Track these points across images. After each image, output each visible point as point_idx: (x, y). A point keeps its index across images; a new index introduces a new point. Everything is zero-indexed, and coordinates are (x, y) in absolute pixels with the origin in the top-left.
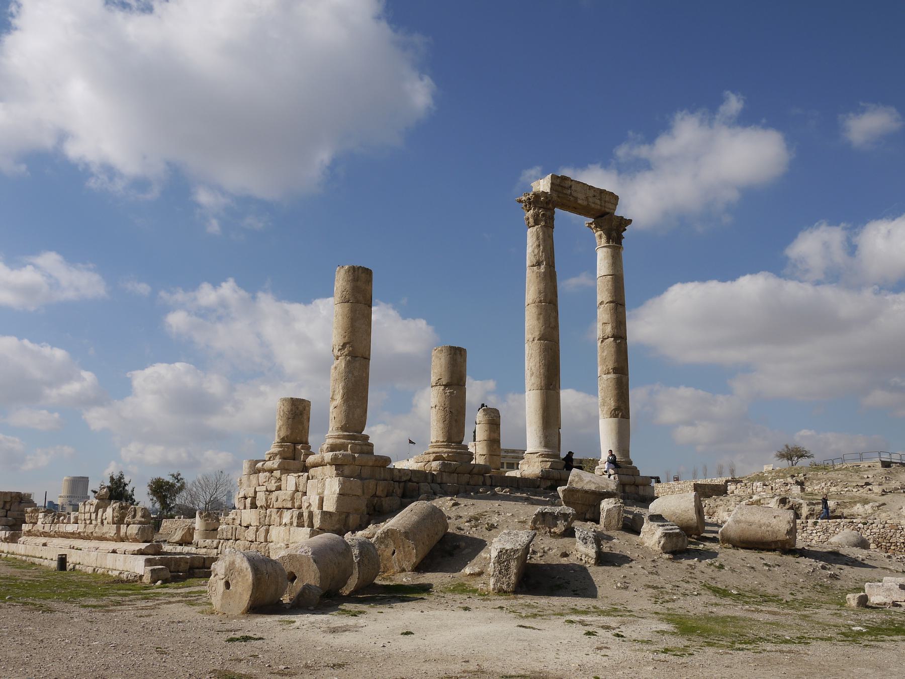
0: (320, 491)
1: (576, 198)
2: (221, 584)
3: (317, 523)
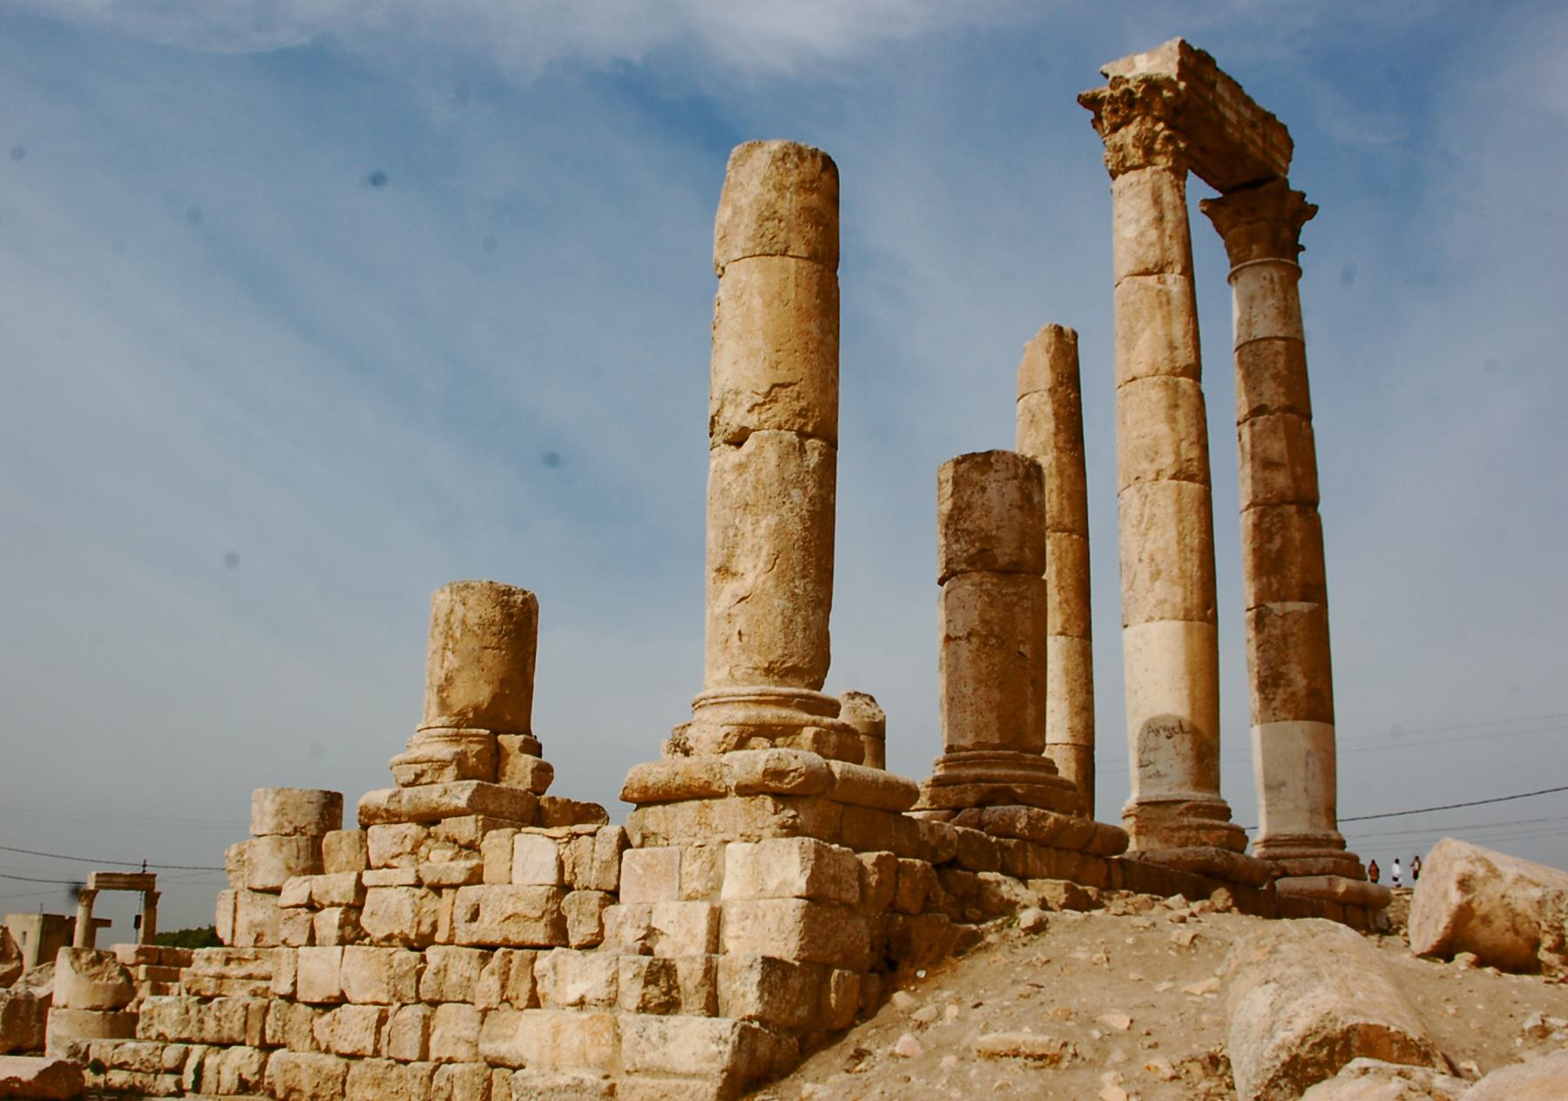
0: (698, 885)
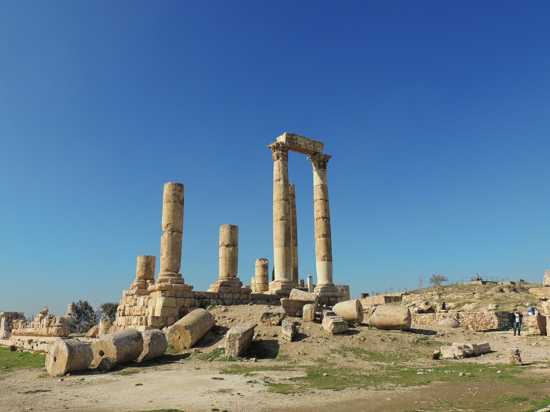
1: (300, 145)
2: (52, 359)
3: (150, 323)
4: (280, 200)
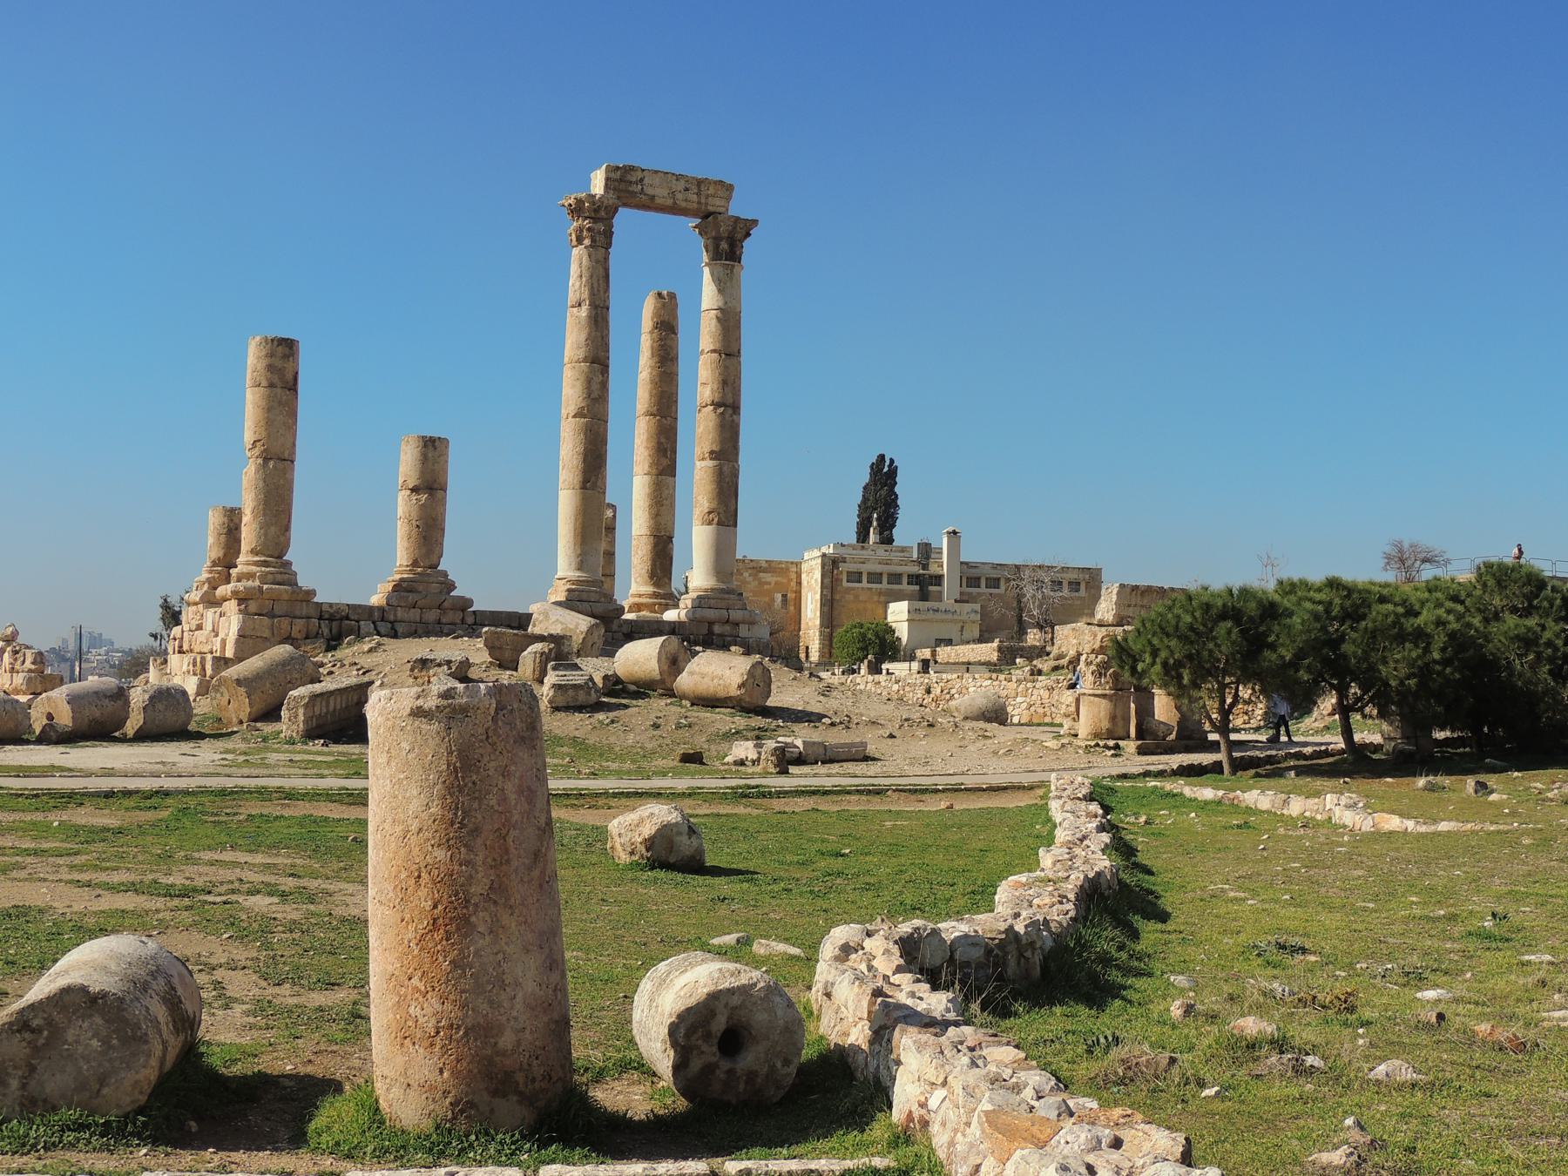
4: (578, 361)
